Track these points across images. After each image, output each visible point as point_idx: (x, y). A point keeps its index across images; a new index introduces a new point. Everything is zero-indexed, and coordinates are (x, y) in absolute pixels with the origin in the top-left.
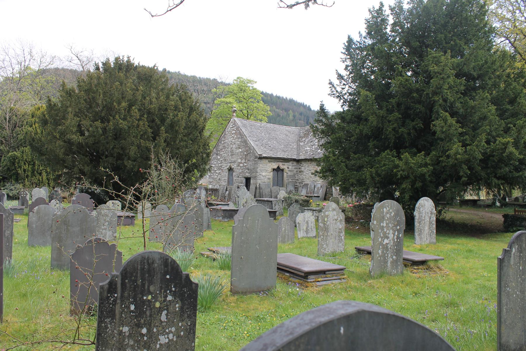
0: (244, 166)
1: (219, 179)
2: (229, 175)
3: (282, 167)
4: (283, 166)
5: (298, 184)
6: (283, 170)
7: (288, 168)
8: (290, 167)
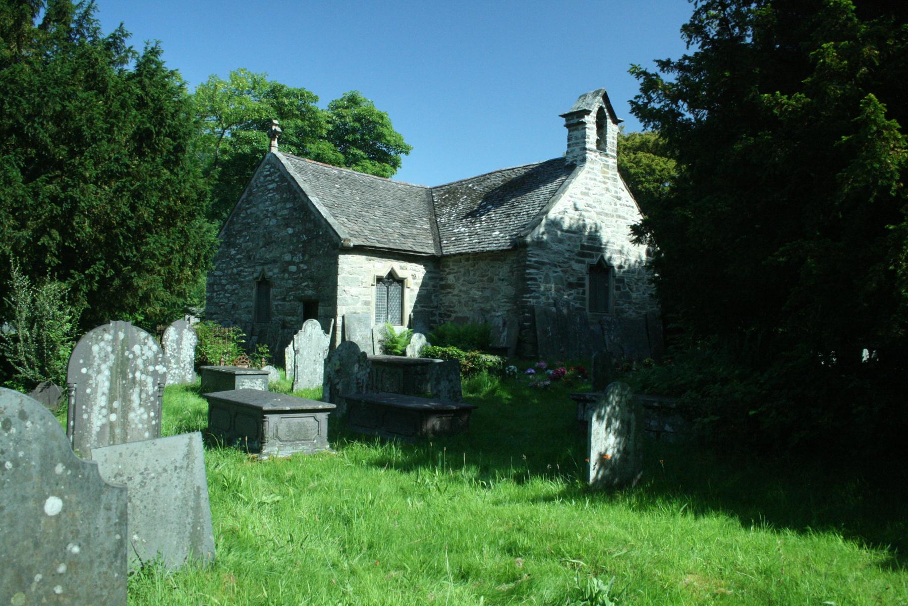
0: (299, 270)
1: (234, 306)
2: (259, 293)
3: (401, 274)
5: (437, 318)
6: (401, 282)
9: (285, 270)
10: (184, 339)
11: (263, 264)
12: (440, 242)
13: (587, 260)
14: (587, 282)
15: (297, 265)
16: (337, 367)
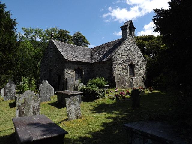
7: (85, 68)
8: (86, 68)
9: (54, 68)
10: (12, 87)
12: (92, 60)
13: (128, 63)
15: (56, 66)
16: (23, 102)
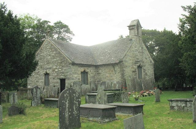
4: (88, 70)
5: (96, 82)
6: (87, 73)
9: (54, 71)
11: (47, 69)
13: (137, 65)
14: (137, 70)
16: (100, 97)
